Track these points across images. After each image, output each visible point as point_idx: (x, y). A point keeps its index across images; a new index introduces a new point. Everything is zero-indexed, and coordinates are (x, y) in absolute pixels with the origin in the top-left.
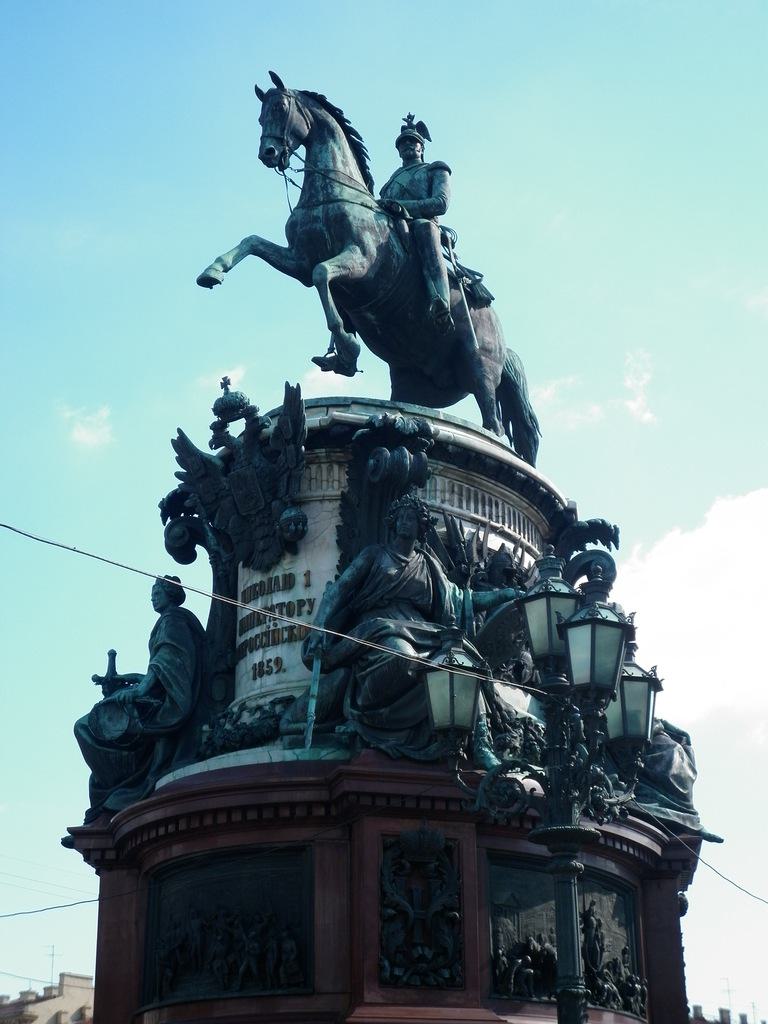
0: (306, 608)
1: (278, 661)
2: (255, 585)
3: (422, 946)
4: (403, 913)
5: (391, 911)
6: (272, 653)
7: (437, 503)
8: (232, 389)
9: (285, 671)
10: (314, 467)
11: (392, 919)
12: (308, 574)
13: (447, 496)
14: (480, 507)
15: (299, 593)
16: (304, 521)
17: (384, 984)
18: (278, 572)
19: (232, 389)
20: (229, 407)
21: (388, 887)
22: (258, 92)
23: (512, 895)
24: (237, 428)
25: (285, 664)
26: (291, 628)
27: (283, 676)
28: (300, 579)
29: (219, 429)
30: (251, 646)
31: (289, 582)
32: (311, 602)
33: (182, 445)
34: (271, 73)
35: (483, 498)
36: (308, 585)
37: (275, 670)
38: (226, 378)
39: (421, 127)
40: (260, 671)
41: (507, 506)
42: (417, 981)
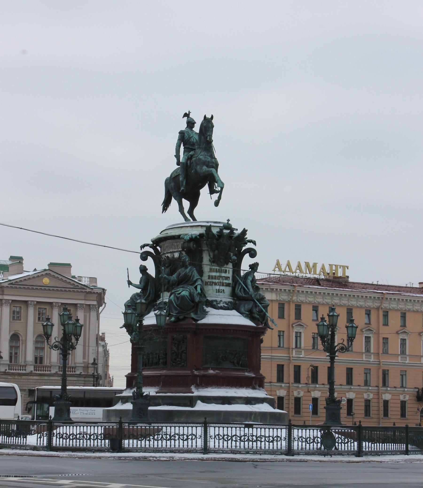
0: (228, 279)
1: (223, 290)
2: (216, 269)
6: (222, 288)
9: (225, 293)
15: (226, 275)
19: (229, 222)
22: (205, 117)
24: (226, 231)
25: (225, 291)
26: (226, 283)
27: (224, 294)
30: (216, 284)
31: (226, 272)
32: (229, 277)
36: (229, 273)
37: (223, 292)
38: (229, 219)
40: (218, 291)
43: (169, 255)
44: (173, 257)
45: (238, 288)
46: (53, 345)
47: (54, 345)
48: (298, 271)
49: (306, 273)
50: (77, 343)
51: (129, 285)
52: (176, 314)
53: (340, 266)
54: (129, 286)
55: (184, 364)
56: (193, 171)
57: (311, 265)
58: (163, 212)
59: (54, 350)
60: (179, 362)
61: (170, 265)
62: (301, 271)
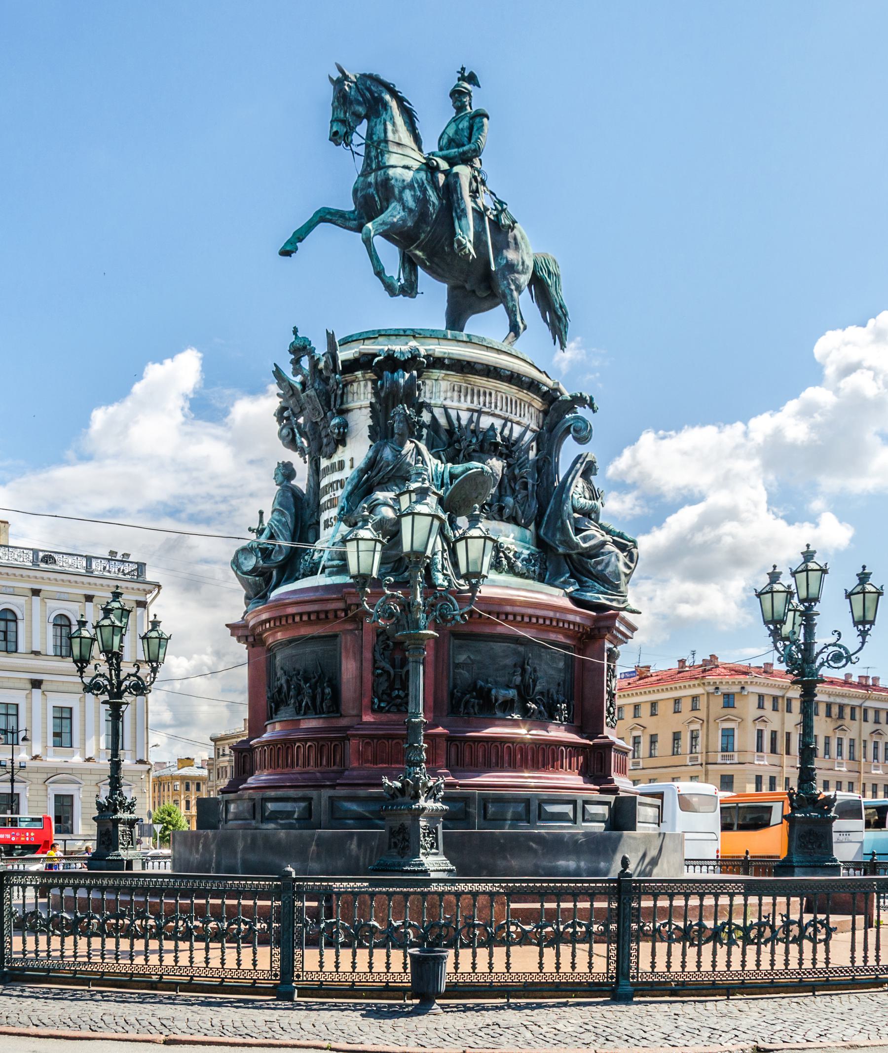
3: (398, 690)
4: (388, 673)
5: (379, 671)
7: (439, 402)
8: (300, 335)
10: (355, 385)
11: (379, 675)
12: (352, 460)
13: (449, 394)
14: (475, 398)
16: (345, 425)
17: (373, 711)
18: (336, 459)
20: (300, 349)
21: (378, 656)
23: (469, 657)
24: (305, 363)
28: (348, 464)
29: (296, 362)
35: (479, 392)
39: (472, 79)
41: (499, 395)
42: (394, 709)
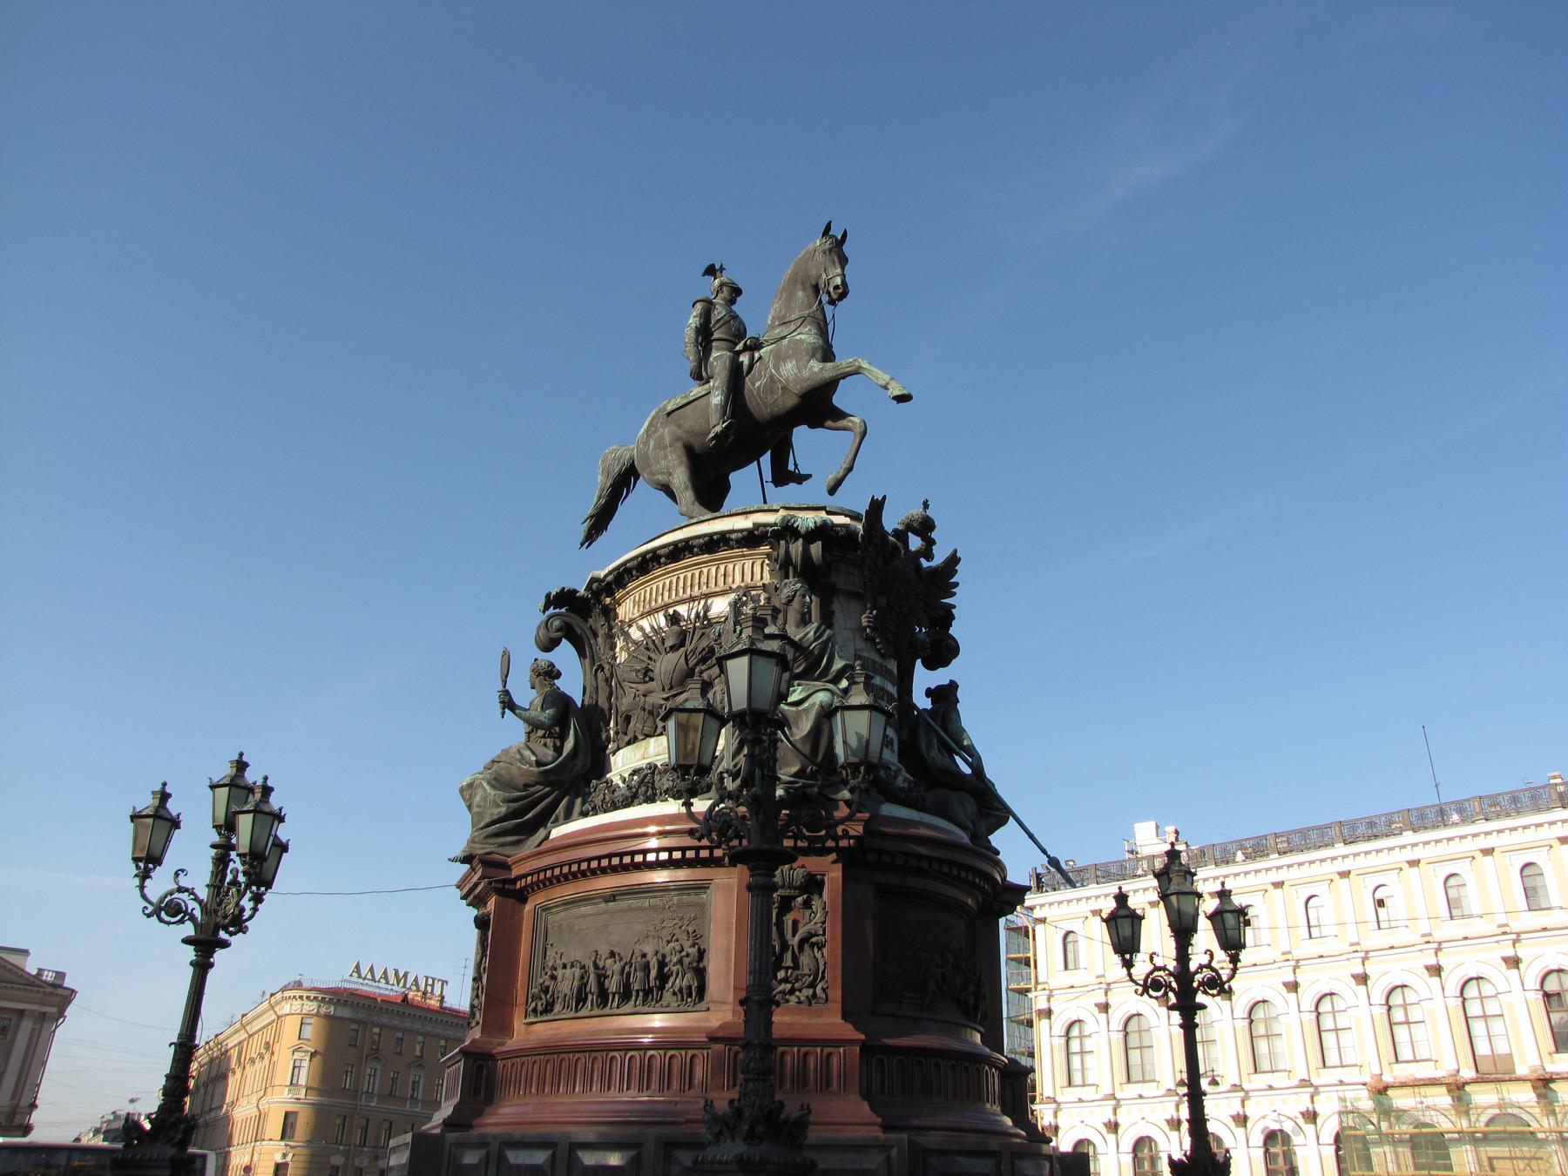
19: (929, 513)
33: (877, 507)
34: (845, 231)
43: (682, 610)
44: (704, 618)
45: (929, 747)
46: (161, 901)
47: (167, 900)
48: (383, 981)
49: (393, 985)
50: (255, 910)
51: (504, 709)
52: (792, 779)
53: (439, 980)
54: (503, 713)
55: (814, 993)
56: (758, 384)
57: (401, 975)
58: (582, 545)
59: (161, 920)
60: (789, 986)
61: (682, 644)
62: (387, 983)
